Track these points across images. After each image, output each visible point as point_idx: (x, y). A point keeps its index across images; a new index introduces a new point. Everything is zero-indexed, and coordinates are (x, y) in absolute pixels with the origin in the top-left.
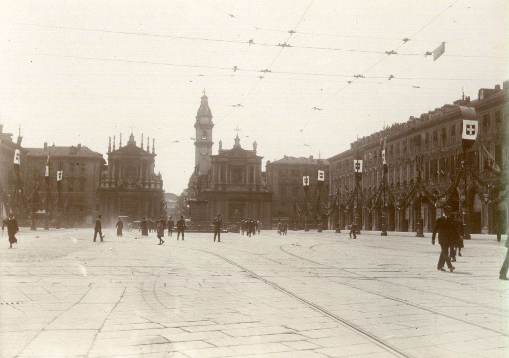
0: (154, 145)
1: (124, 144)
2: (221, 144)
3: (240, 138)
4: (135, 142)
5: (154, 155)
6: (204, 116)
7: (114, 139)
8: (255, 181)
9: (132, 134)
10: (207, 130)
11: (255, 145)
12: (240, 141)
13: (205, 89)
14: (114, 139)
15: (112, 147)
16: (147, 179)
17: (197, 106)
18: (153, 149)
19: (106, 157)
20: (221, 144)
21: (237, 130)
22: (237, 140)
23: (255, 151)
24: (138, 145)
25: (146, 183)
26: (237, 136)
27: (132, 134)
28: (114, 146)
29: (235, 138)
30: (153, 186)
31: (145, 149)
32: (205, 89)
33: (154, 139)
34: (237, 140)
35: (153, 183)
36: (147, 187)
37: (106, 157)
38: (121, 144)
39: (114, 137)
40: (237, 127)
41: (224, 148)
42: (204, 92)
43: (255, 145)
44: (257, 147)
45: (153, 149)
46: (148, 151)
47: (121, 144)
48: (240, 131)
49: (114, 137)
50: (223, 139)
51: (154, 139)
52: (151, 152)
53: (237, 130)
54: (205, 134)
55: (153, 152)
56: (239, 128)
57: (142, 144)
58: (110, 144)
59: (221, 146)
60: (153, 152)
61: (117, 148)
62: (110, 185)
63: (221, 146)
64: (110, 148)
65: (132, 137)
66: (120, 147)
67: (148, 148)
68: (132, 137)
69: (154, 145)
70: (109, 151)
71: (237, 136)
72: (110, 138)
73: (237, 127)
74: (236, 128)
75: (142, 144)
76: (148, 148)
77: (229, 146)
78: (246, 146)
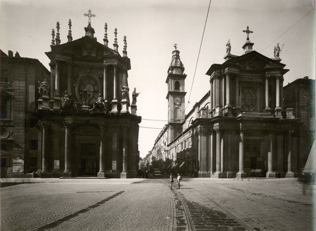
10: (179, 81)
16: (114, 97)
17: (168, 61)
18: (125, 52)
19: (46, 62)
21: (248, 32)
25: (115, 103)
30: (124, 109)
32: (176, 45)
33: (125, 38)
35: (124, 103)
36: (115, 110)
37: (46, 62)
40: (248, 28)
42: (175, 47)
45: (125, 52)
54: (177, 86)
56: (250, 29)
57: (106, 40)
59: (229, 50)
62: (51, 104)
63: (229, 50)
73: (248, 28)
74: (246, 29)
76: (116, 45)
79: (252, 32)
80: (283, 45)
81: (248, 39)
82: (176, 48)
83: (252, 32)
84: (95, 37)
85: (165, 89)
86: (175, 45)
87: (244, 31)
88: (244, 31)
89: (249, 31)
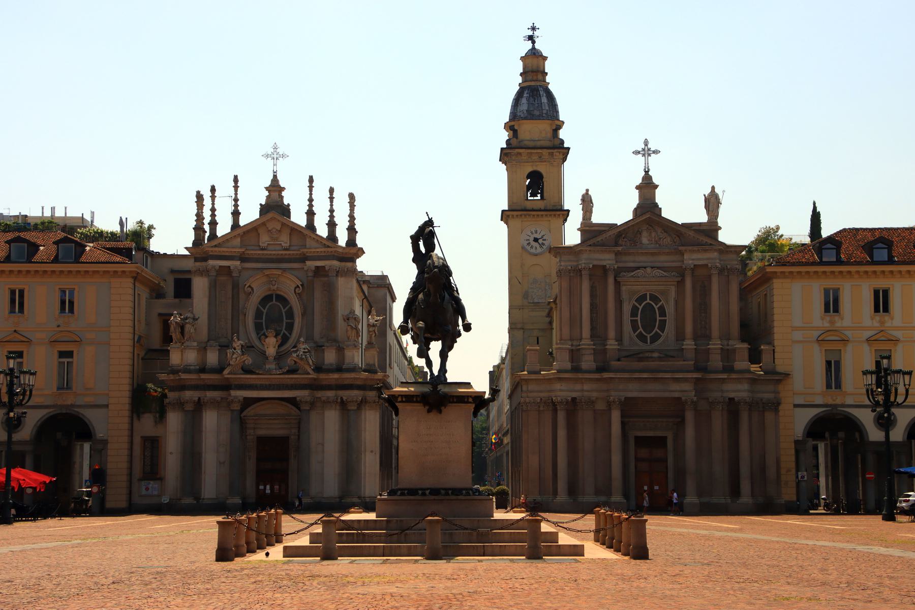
0: (352, 218)
1: (250, 214)
2: (587, 202)
3: (655, 180)
4: (285, 211)
5: (353, 251)
6: (530, 116)
7: (213, 197)
8: (715, 332)
9: (275, 179)
10: (541, 168)
11: (712, 202)
12: (657, 191)
13: (534, 29)
14: (213, 197)
15: (207, 227)
18: (352, 230)
20: (587, 202)
21: (646, 152)
22: (647, 187)
23: (710, 229)
24: (299, 217)
26: (647, 178)
27: (275, 179)
28: (213, 224)
29: (639, 181)
31: (322, 230)
32: (534, 29)
33: (352, 197)
34: (647, 187)
38: (236, 214)
39: (213, 189)
40: (646, 143)
41: (598, 218)
42: (531, 38)
43: (712, 202)
44: (722, 210)
45: (352, 230)
46: (332, 237)
47: (236, 214)
48: (653, 158)
49: (213, 189)
50: (598, 186)
51: (352, 197)
52: (342, 238)
53: (646, 152)
54: (536, 182)
55: (352, 242)
56: (652, 146)
57: (311, 214)
58: (199, 217)
60: (352, 242)
61: (224, 228)
64: (199, 229)
65: (275, 188)
66: (235, 225)
67: (332, 225)
68: (275, 188)
69: (352, 218)
70: (198, 242)
71: (647, 178)
72: (200, 197)
73: (646, 143)
75: (311, 214)
76: (332, 225)
77: (616, 209)
78: (680, 207)
79: (656, 152)
80: (724, 191)
81: (647, 172)
82: (534, 42)
83: (656, 152)
84: (286, 203)
85: (495, 186)
86: (530, 33)
87: (637, 153)
88: (637, 153)
89: (649, 150)
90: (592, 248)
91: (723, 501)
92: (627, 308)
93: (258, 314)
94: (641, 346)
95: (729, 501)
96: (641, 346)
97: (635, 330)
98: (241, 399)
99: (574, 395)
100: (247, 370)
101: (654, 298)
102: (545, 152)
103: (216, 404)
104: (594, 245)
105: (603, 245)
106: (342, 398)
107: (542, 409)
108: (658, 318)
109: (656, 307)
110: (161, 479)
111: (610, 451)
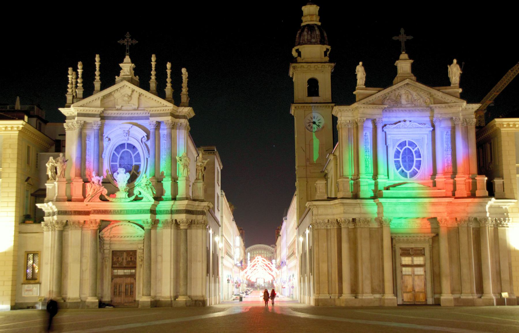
90: (365, 106)
91: (470, 297)
92: (392, 153)
93: (113, 159)
94: (402, 179)
95: (475, 296)
96: (402, 179)
97: (398, 169)
98: (98, 221)
99: (354, 216)
100: (103, 199)
101: (411, 144)
102: (320, 65)
103: (82, 225)
104: (367, 103)
105: (373, 104)
106: (176, 220)
107: (329, 228)
108: (415, 159)
109: (413, 151)
110: (40, 283)
111: (382, 259)
